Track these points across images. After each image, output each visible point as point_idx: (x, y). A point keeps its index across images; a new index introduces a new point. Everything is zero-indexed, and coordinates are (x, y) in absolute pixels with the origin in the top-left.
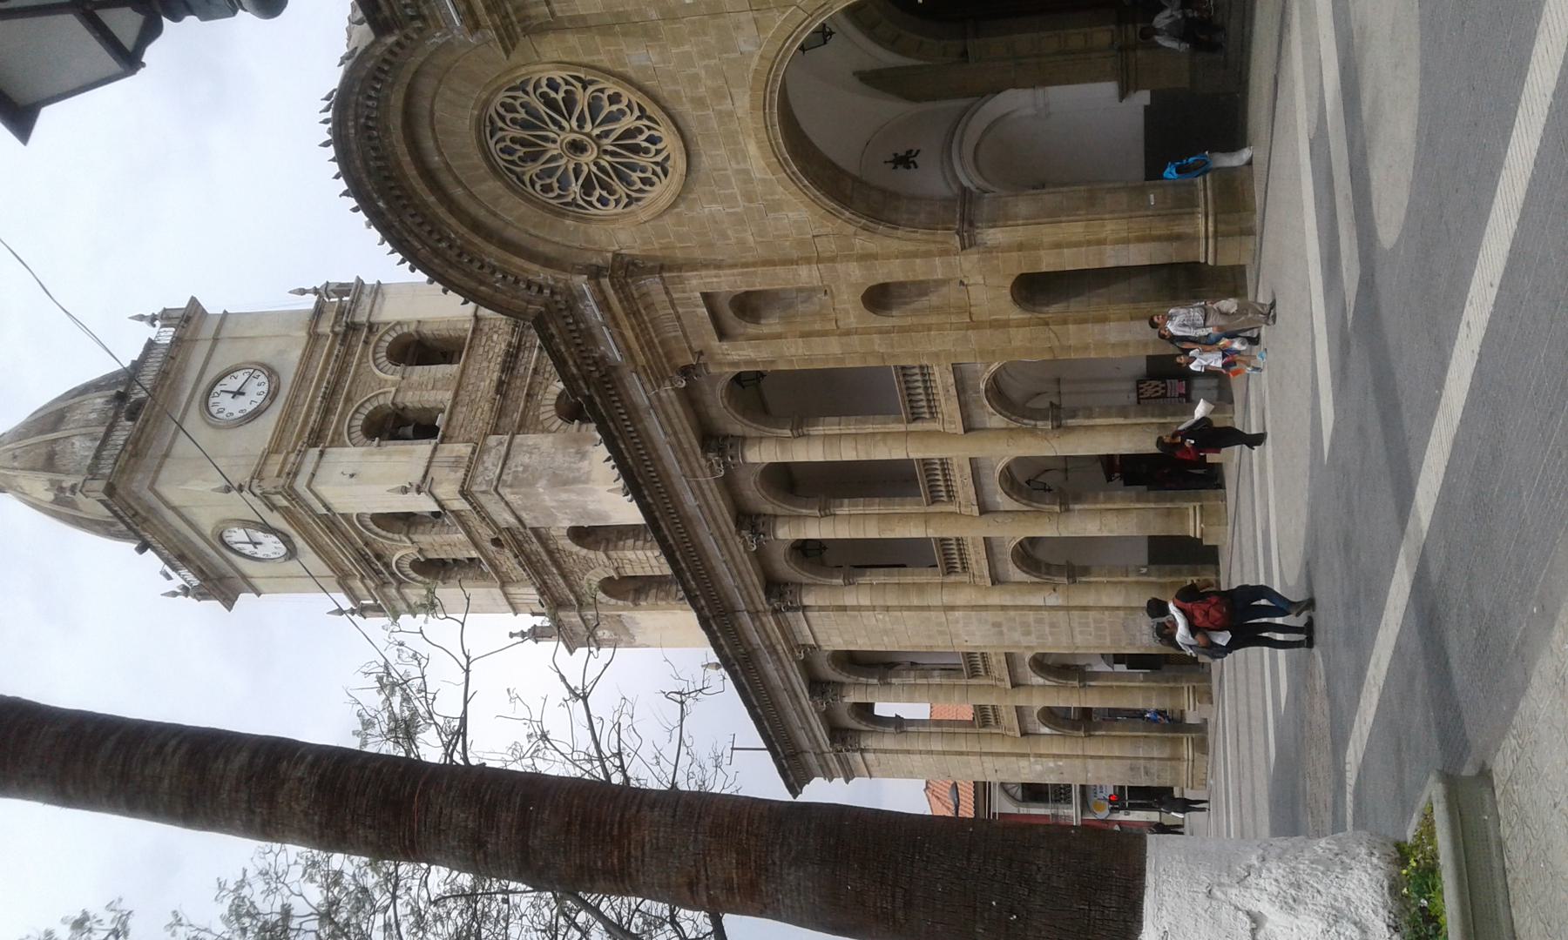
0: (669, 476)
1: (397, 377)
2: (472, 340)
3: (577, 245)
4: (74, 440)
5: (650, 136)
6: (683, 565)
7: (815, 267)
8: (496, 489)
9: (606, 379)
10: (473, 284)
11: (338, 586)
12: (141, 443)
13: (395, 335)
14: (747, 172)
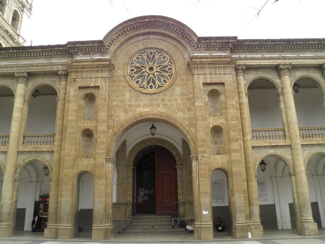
0: (17, 60)
1: (12, 9)
2: (15, 32)
3: (119, 60)
5: (152, 87)
9: (67, 53)
10: (116, 31)
13: (20, 15)
14: (139, 106)
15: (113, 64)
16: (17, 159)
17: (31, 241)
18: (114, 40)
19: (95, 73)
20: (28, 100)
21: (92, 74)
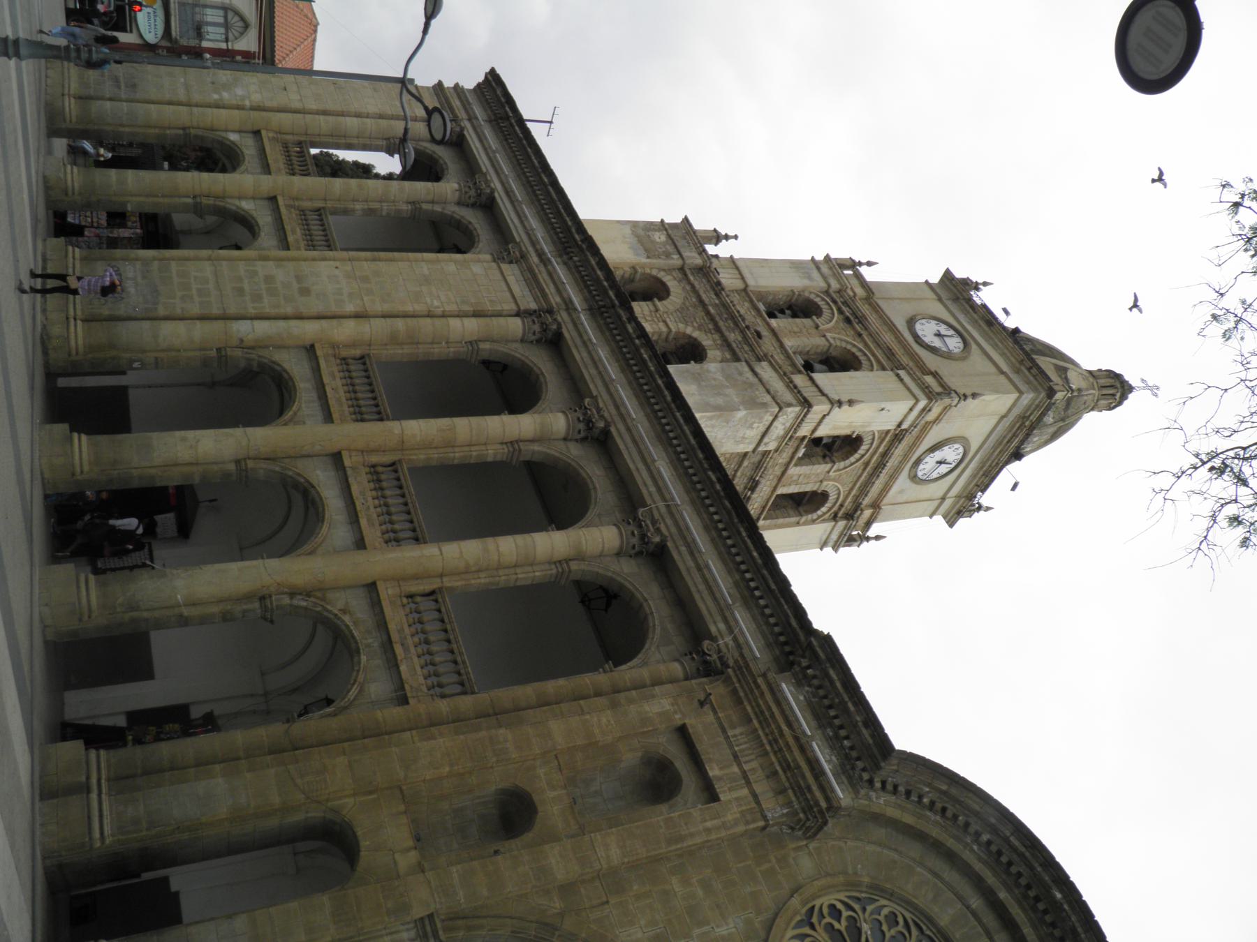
0: (693, 502)
1: (825, 483)
2: (761, 514)
3: (850, 843)
4: (1051, 420)
6: (660, 382)
7: (605, 866)
8: (781, 409)
9: (787, 649)
10: (954, 791)
11: (874, 290)
12: (1018, 425)
13: (819, 513)
15: (825, 823)
16: (345, 588)
17: (29, 690)
18: (914, 798)
19: (763, 770)
20: (570, 571)
21: (753, 757)
